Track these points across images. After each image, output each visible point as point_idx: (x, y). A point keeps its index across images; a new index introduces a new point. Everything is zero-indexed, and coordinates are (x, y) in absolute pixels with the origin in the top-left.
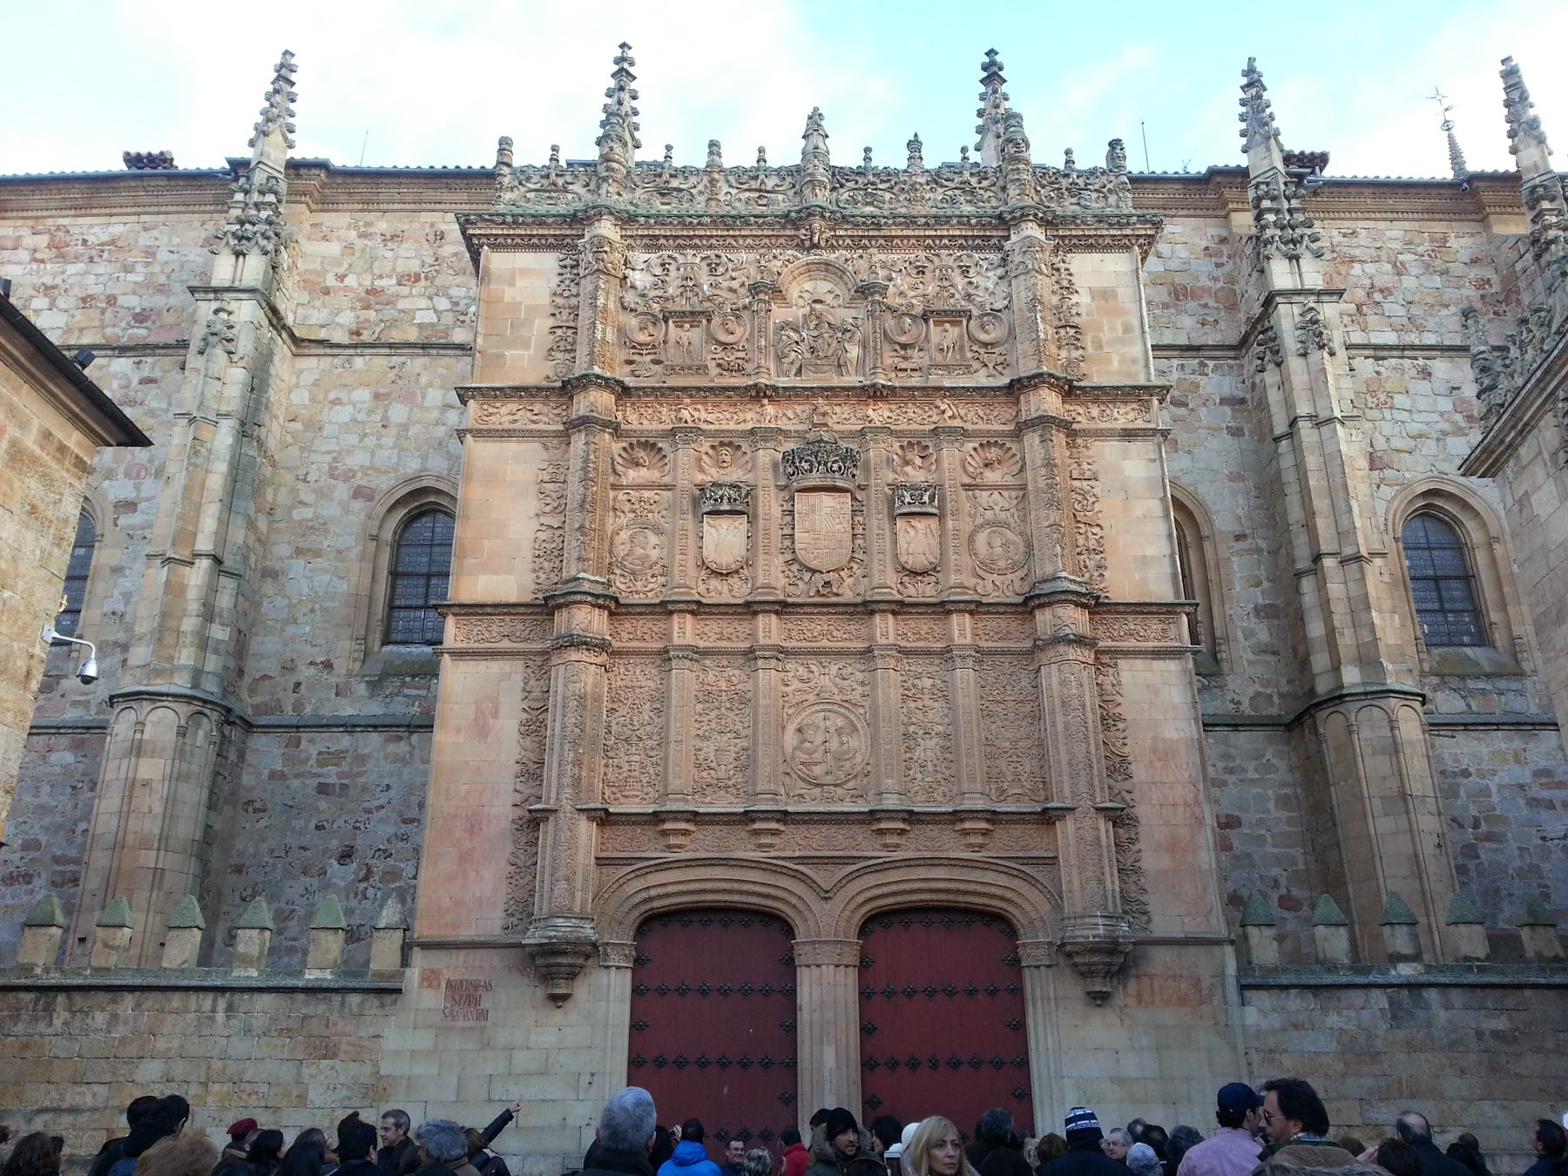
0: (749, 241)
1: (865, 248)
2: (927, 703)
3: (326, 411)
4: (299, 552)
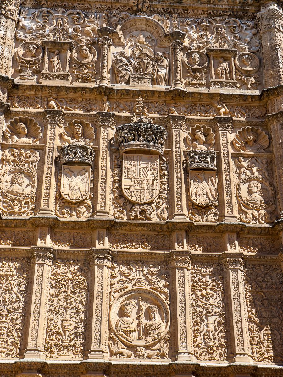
1: (170, 14)
2: (209, 291)
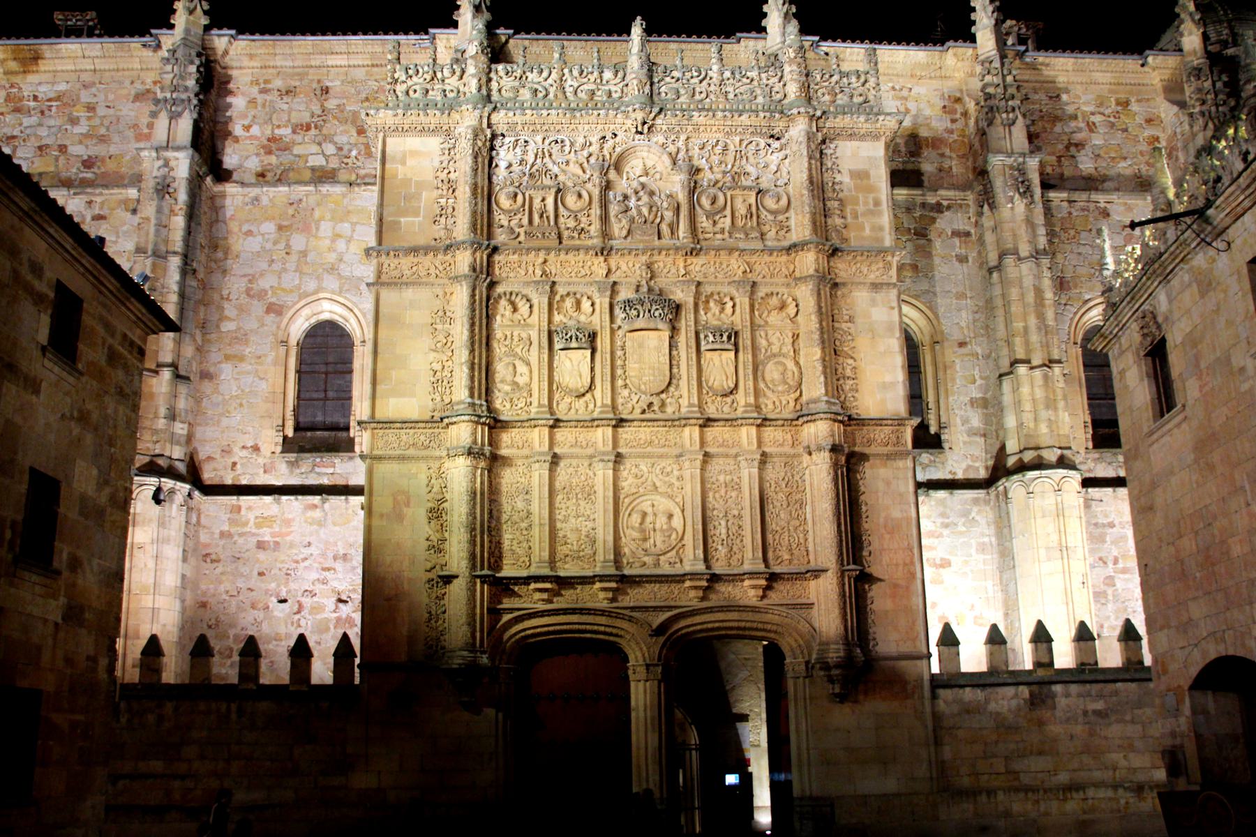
0: (587, 127)
3: (241, 241)
4: (228, 358)
